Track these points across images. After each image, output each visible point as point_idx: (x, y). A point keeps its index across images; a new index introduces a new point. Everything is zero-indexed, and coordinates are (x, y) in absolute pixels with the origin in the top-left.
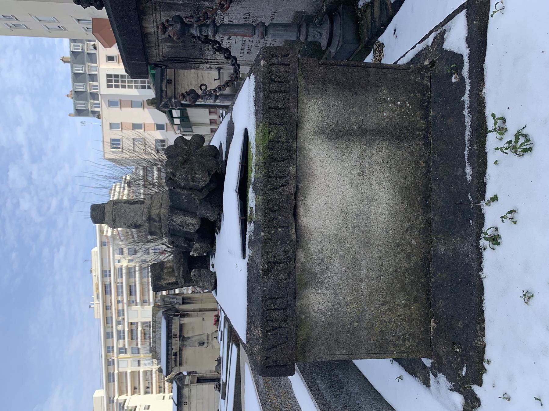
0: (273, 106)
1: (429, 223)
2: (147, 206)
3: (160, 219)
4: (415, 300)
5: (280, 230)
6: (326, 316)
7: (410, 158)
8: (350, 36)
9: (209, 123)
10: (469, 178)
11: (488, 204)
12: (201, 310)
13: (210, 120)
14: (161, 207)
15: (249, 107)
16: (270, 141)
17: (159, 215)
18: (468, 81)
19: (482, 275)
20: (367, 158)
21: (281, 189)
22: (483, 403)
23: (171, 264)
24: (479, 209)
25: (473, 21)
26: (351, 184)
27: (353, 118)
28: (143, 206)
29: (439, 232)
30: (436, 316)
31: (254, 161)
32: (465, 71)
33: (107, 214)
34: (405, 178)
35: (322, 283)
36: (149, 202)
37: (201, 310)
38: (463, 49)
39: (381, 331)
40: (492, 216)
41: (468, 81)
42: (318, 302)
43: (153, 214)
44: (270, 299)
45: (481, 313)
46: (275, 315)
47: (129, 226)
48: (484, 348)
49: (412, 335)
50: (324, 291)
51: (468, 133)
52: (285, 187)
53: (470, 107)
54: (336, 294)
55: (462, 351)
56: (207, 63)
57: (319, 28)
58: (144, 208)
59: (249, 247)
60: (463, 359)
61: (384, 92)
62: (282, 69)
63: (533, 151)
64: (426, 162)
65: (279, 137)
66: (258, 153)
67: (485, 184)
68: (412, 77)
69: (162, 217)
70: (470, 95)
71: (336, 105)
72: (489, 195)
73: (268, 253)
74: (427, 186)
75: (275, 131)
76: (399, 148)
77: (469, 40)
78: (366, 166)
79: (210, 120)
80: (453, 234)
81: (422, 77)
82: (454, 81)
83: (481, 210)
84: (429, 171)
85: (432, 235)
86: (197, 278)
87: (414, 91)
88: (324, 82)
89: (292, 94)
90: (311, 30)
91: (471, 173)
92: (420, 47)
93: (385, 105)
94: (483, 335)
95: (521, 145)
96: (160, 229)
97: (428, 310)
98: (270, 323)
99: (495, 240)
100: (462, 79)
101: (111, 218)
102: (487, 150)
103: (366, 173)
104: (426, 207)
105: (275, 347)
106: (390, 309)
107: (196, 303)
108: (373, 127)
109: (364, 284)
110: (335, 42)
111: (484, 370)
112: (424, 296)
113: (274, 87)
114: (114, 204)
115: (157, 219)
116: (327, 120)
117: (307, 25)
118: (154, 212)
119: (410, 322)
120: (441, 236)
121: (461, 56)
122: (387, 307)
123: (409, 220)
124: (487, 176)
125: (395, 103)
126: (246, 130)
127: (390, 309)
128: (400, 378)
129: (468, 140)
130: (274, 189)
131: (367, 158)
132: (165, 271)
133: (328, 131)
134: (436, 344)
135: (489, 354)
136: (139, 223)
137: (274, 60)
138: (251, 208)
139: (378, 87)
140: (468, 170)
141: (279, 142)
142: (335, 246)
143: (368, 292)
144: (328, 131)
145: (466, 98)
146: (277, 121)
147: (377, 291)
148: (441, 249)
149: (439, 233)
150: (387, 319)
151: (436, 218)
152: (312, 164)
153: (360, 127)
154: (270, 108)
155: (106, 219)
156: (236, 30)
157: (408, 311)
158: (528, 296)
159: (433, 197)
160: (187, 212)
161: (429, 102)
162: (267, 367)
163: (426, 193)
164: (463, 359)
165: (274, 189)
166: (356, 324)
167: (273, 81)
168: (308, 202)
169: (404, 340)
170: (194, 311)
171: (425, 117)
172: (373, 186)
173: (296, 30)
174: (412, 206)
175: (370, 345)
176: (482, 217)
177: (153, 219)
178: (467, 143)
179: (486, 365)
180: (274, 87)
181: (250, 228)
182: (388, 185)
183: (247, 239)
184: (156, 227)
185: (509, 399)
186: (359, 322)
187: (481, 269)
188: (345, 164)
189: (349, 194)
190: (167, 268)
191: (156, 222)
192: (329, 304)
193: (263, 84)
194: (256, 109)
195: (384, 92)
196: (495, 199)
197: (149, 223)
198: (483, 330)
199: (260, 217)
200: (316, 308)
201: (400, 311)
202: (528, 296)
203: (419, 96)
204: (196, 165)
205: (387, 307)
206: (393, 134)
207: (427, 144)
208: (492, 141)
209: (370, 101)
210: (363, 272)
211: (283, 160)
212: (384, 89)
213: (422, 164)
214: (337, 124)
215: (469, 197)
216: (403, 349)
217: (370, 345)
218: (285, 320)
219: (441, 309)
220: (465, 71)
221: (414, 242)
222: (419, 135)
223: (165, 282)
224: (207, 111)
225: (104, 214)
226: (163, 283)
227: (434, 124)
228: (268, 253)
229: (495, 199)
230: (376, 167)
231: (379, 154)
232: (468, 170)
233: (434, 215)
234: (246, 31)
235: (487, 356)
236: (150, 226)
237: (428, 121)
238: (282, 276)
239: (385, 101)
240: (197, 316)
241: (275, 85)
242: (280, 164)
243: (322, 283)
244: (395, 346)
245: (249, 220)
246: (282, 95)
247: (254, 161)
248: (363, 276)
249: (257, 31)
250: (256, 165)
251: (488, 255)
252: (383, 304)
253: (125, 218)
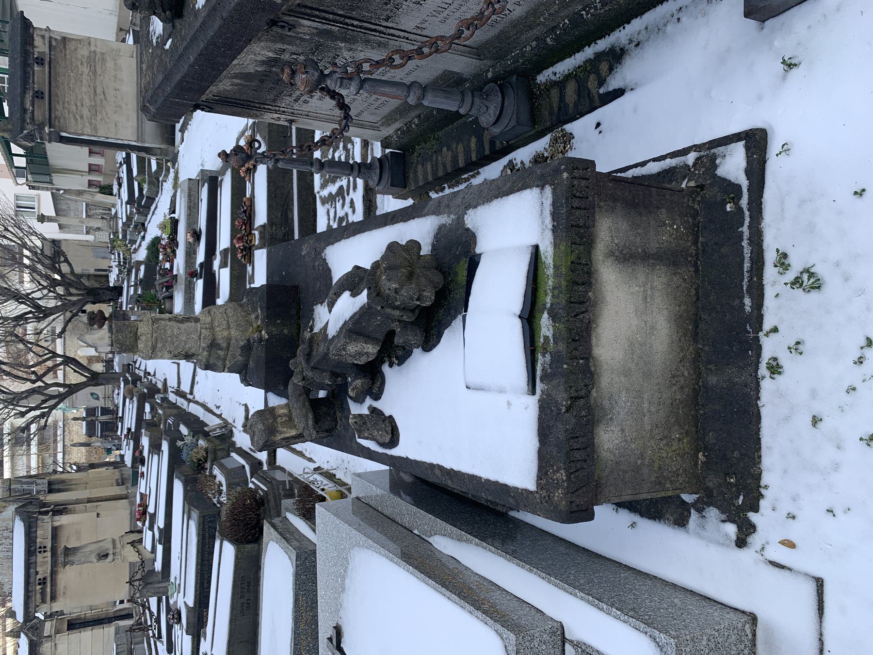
0: (574, 223)
1: (698, 354)
2: (207, 326)
3: (229, 345)
4: (687, 433)
6: (614, 455)
7: (684, 285)
8: (525, 116)
10: (748, 309)
11: (767, 335)
12: (90, 501)
13: (90, 165)
14: (229, 328)
15: (543, 222)
16: (572, 262)
17: (229, 340)
18: (747, 213)
19: (760, 403)
20: (649, 284)
21: (581, 316)
22: (759, 528)
23: (285, 411)
24: (757, 339)
25: (753, 154)
26: (636, 311)
27: (638, 240)
28: (199, 325)
29: (709, 362)
30: (706, 449)
31: (550, 283)
32: (744, 202)
33: (143, 338)
34: (680, 306)
35: (611, 419)
36: (208, 319)
37: (90, 501)
38: (743, 182)
39: (660, 468)
40: (770, 347)
41: (747, 213)
42: (609, 439)
43: (220, 337)
44: (572, 438)
45: (759, 439)
46: (577, 455)
47: (175, 357)
48: (760, 474)
49: (685, 470)
50: (613, 428)
51: (747, 265)
52: (585, 315)
53: (749, 239)
54: (623, 430)
55: (737, 481)
56: (276, 112)
57: (487, 100)
58: (201, 328)
59: (542, 380)
60: (738, 489)
61: (663, 214)
62: (583, 183)
63: (822, 288)
64: (696, 289)
65: (579, 258)
66: (556, 275)
67: (763, 315)
68: (686, 200)
69: (233, 341)
70: (749, 227)
71: (624, 226)
72: (767, 326)
73: (571, 387)
74: (697, 314)
75: (577, 252)
76: (675, 274)
77: (748, 172)
78: (649, 293)
79: (90, 165)
80: (728, 364)
81: (694, 201)
82: (728, 209)
83: (759, 341)
84: (698, 299)
85: (701, 366)
86: (361, 426)
87: (686, 216)
88: (615, 200)
89: (590, 211)
90: (477, 101)
91: (750, 304)
92: (669, 163)
93: (664, 228)
94: (760, 462)
95: (809, 281)
96: (225, 359)
97: (699, 443)
98: (572, 464)
99: (775, 369)
100: (740, 209)
101: (150, 344)
102: (765, 282)
103: (649, 299)
104: (696, 336)
105: (577, 490)
106: (667, 444)
107: (75, 490)
108: (655, 251)
109: (646, 418)
110: (504, 121)
111: (761, 496)
112: (694, 429)
113: (576, 203)
114: (153, 322)
115: (224, 345)
116: (616, 241)
117: (473, 96)
118: (221, 334)
119: (682, 457)
120: (712, 367)
121: (739, 187)
122: (665, 442)
123: (682, 350)
124: (764, 307)
125: (672, 226)
126: (536, 248)
127: (667, 444)
128: (633, 525)
129: (748, 272)
130: (576, 316)
131: (649, 284)
132: (279, 420)
133: (617, 254)
134: (704, 478)
135: (766, 479)
136: (193, 351)
137: (576, 173)
138: (546, 338)
139: (658, 208)
140: (747, 301)
141: (580, 264)
142: (623, 379)
143: (649, 427)
144: (617, 254)
145: (745, 229)
146: (578, 240)
147: (657, 425)
148: (713, 380)
149: (710, 364)
150: (665, 455)
151: (706, 348)
152: (603, 289)
153: (644, 251)
154: (572, 226)
155: (141, 346)
156: (387, 90)
157: (681, 446)
158: (816, 421)
159: (702, 326)
160: (369, 337)
161: (698, 227)
162: (571, 512)
163: (696, 321)
164: (738, 489)
165: (576, 316)
166: (639, 462)
167: (575, 196)
168: (600, 330)
169: (678, 475)
170: (78, 502)
171: (695, 242)
172: (654, 314)
173: (459, 98)
174: (685, 335)
175: (651, 483)
176: (760, 347)
177: (218, 345)
178: (746, 275)
179: (763, 491)
180: (576, 203)
181: (542, 361)
182: (665, 312)
183: (539, 373)
184: (219, 357)
185: (794, 518)
186: (642, 460)
187: (759, 398)
188: (632, 290)
189: (635, 322)
190: (280, 416)
191: (221, 349)
192: (617, 442)
193: (567, 199)
194: (553, 226)
195: (663, 214)
196: (775, 330)
197: (210, 352)
198: (760, 457)
199: (562, 347)
200: (606, 447)
201: (675, 445)
202: (816, 421)
203: (690, 220)
204: (423, 279)
205: (665, 442)
206: (669, 258)
207: (697, 271)
208: (770, 272)
209: (653, 223)
210: (646, 405)
211: (583, 284)
212: (664, 211)
213: (693, 292)
214: (624, 246)
215: (748, 328)
216: (677, 485)
217: (651, 483)
218: (585, 461)
219: (713, 441)
220: (744, 202)
221: (686, 374)
222: (689, 262)
223: (282, 436)
224: (86, 150)
225: (136, 338)
226: (279, 437)
227: (703, 251)
228: (571, 387)
229: (775, 330)
230: (657, 294)
231: (659, 279)
232: (747, 301)
233: (703, 345)
234: (400, 92)
235: (763, 483)
236: (209, 355)
237: (697, 247)
238: (583, 413)
239: (665, 224)
240: (86, 511)
241: (577, 200)
242: (581, 288)
243: (611, 419)
244: (671, 482)
245: (541, 350)
246: (582, 212)
247: (550, 283)
248: (645, 410)
249: (412, 94)
250: (554, 288)
251: (767, 386)
252: (661, 439)
253: (173, 343)
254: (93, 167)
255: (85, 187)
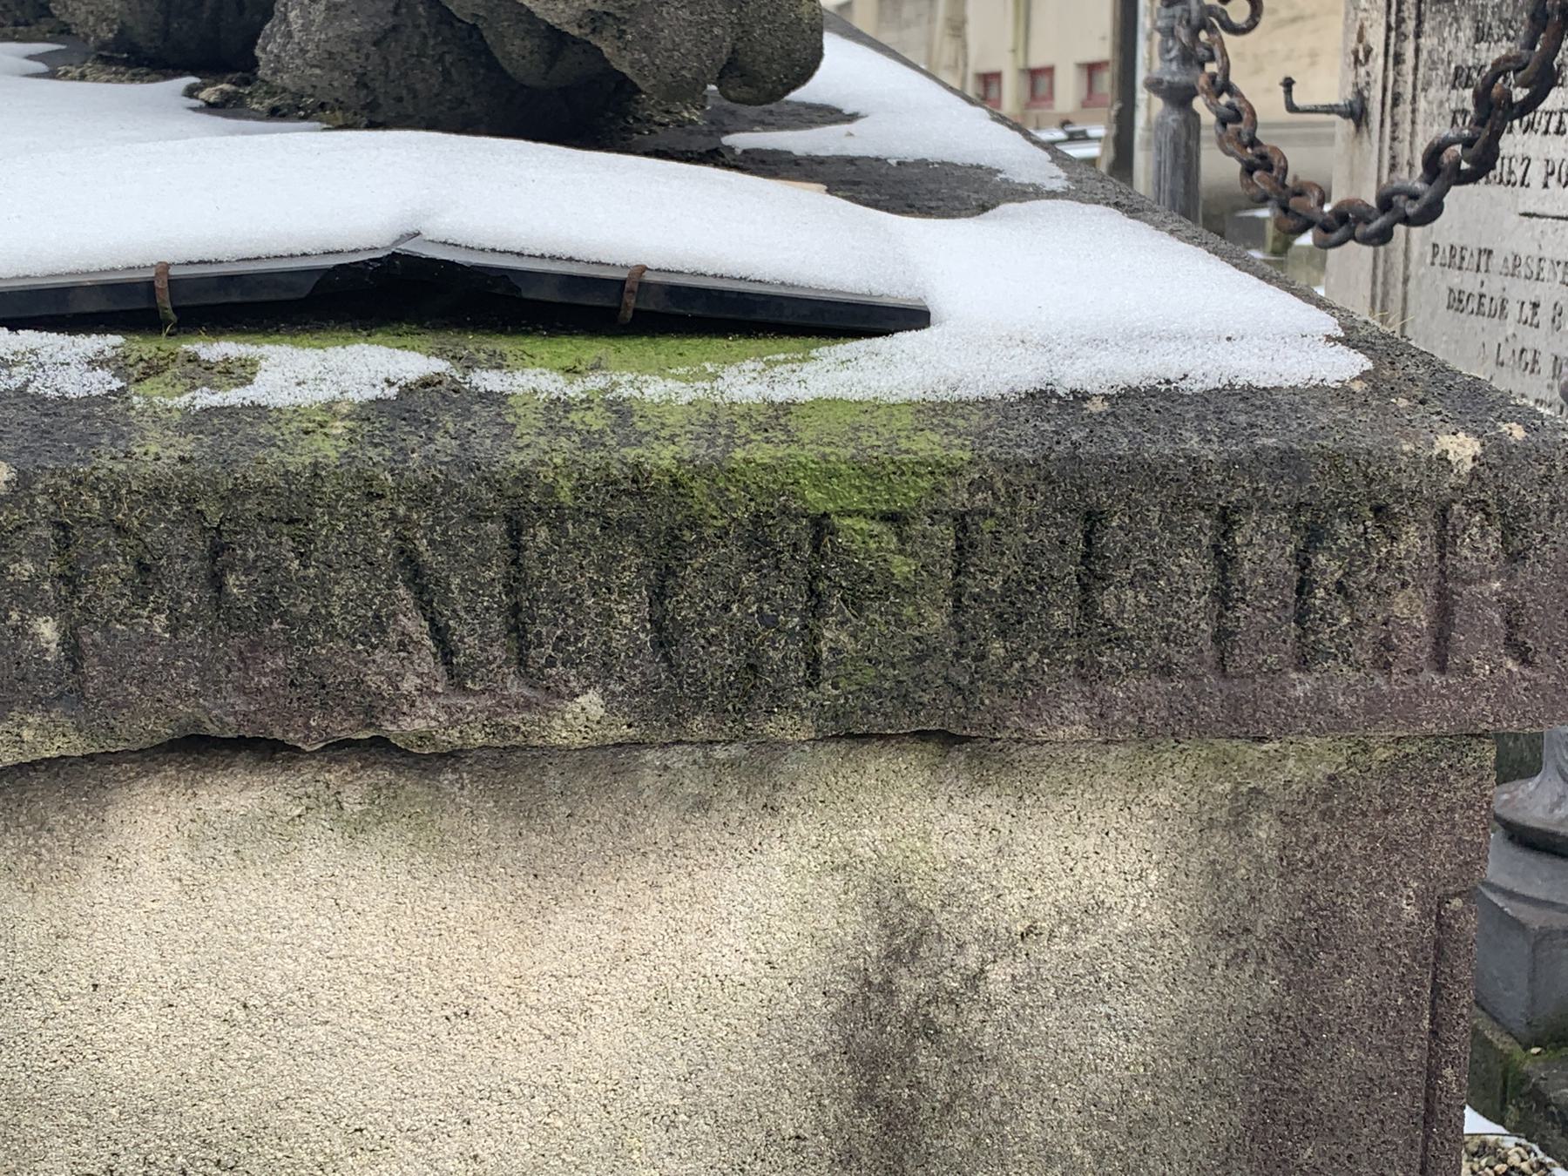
0: (1113, 537)
5: (47, 630)
9: (1036, 62)
13: (1049, 71)
15: (1097, 342)
16: (821, 525)
21: (414, 625)
31: (656, 389)
52: (426, 660)
56: (1394, 28)
62: (1411, 609)
65: (855, 602)
66: (717, 422)
75: (902, 567)
79: (1049, 71)
88: (1306, 946)
113: (1264, 548)
116: (998, 977)
126: (915, 318)
133: (911, 985)
137: (1478, 544)
141: (816, 605)
144: (911, 985)
152: (637, 873)
154: (1093, 519)
165: (409, 561)
167: (1315, 536)
168: (320, 850)
181: (69, 364)
193: (1287, 458)
199: (158, 452)
211: (665, 637)
214: (972, 1056)
224: (1101, 49)
242: (630, 615)
245: (146, 347)
246: (1196, 611)
247: (656, 389)
250: (621, 411)
254: (1043, 81)
255: (979, 62)
